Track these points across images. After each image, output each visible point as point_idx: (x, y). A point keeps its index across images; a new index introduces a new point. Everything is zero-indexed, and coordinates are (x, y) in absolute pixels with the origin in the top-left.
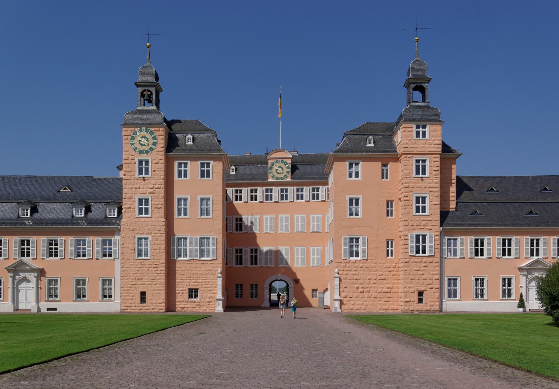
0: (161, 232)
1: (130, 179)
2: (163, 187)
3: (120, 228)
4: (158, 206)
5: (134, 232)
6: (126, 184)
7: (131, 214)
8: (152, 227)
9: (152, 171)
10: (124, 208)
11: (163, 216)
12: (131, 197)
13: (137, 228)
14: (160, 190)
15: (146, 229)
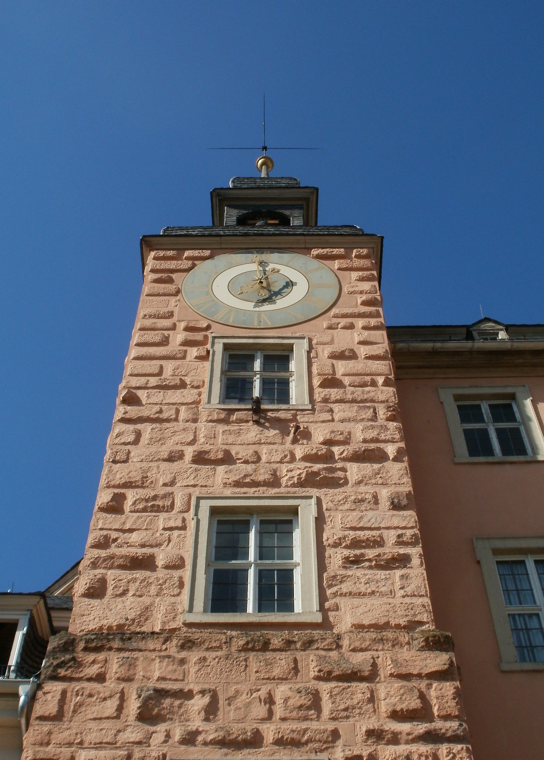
0: (421, 728)
1: (168, 420)
2: (399, 451)
3: (32, 699)
4: (370, 553)
5: (162, 728)
6: (131, 438)
7: (147, 601)
8: (333, 684)
9: (316, 382)
10: (94, 565)
11: (425, 617)
12: (160, 503)
13: (189, 695)
14: (376, 466)
15: (278, 698)
